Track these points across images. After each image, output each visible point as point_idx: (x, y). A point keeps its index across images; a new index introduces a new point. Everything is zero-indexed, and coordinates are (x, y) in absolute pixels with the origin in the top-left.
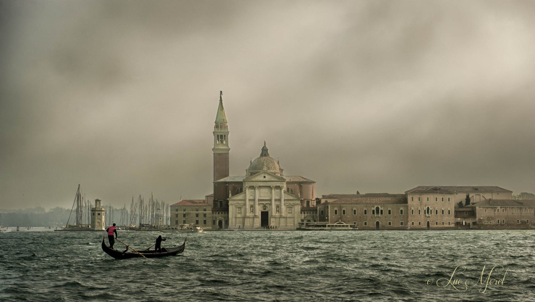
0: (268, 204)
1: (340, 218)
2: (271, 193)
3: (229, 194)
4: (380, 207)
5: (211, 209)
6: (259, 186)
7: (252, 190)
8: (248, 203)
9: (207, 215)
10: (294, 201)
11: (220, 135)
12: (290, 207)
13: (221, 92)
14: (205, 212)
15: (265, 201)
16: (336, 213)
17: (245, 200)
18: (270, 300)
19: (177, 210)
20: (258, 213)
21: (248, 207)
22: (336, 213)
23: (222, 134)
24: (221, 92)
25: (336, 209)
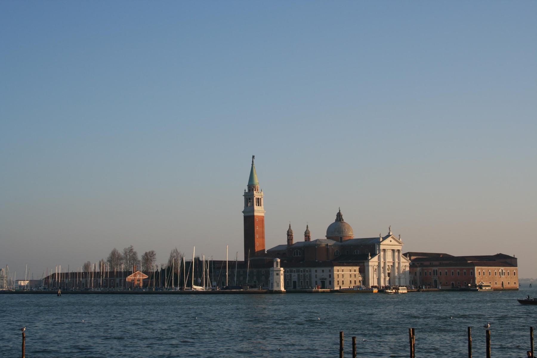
0: (391, 266)
1: (482, 279)
3: (368, 256)
4: (503, 269)
5: (358, 270)
9: (356, 276)
10: (406, 263)
11: (258, 198)
13: (253, 157)
14: (355, 273)
15: (390, 263)
18: (325, 356)
20: (387, 275)
21: (381, 268)
22: (479, 275)
23: (258, 197)
24: (253, 157)
25: (479, 271)
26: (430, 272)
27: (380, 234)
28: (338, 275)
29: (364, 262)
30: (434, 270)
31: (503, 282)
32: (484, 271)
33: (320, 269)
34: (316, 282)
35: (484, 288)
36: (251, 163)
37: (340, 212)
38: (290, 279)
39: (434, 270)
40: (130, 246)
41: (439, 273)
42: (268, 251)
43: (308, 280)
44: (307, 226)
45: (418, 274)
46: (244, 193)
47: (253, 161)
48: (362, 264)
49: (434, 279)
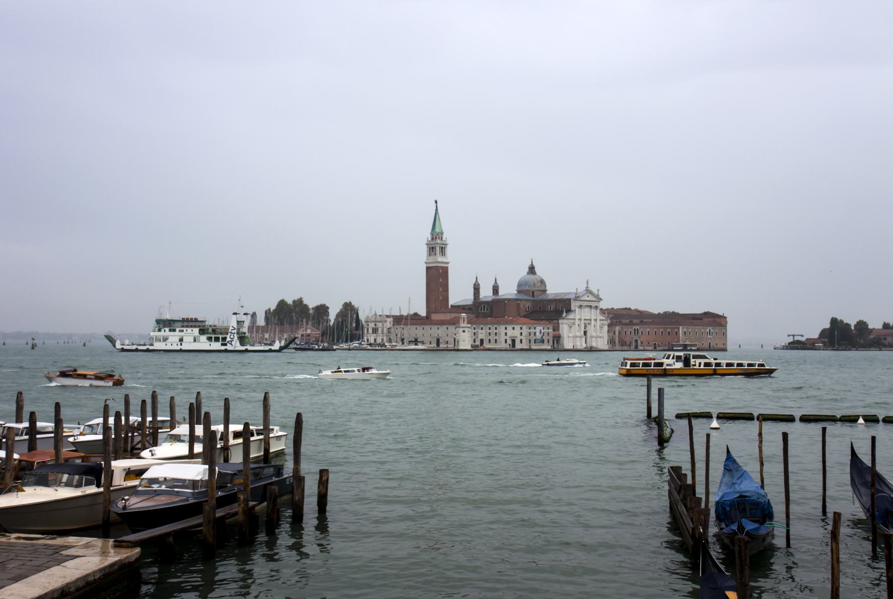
1: (688, 339)
2: (591, 312)
3: (562, 312)
5: (552, 328)
6: (586, 306)
7: (579, 309)
8: (577, 322)
9: (550, 334)
12: (601, 328)
13: (436, 202)
16: (685, 334)
17: (574, 319)
19: (530, 329)
20: (583, 333)
22: (685, 334)
24: (436, 202)
25: (685, 330)
26: (630, 332)
27: (577, 289)
28: (530, 333)
29: (558, 320)
30: (635, 329)
31: (710, 343)
32: (690, 330)
33: (510, 327)
34: (506, 340)
35: (689, 348)
36: (435, 209)
37: (533, 263)
38: (477, 337)
39: (635, 329)
40: (299, 298)
41: (640, 332)
42: (452, 306)
43: (496, 338)
44: (496, 279)
45: (617, 333)
46: (427, 241)
47: (437, 206)
48: (555, 321)
49: (634, 339)
